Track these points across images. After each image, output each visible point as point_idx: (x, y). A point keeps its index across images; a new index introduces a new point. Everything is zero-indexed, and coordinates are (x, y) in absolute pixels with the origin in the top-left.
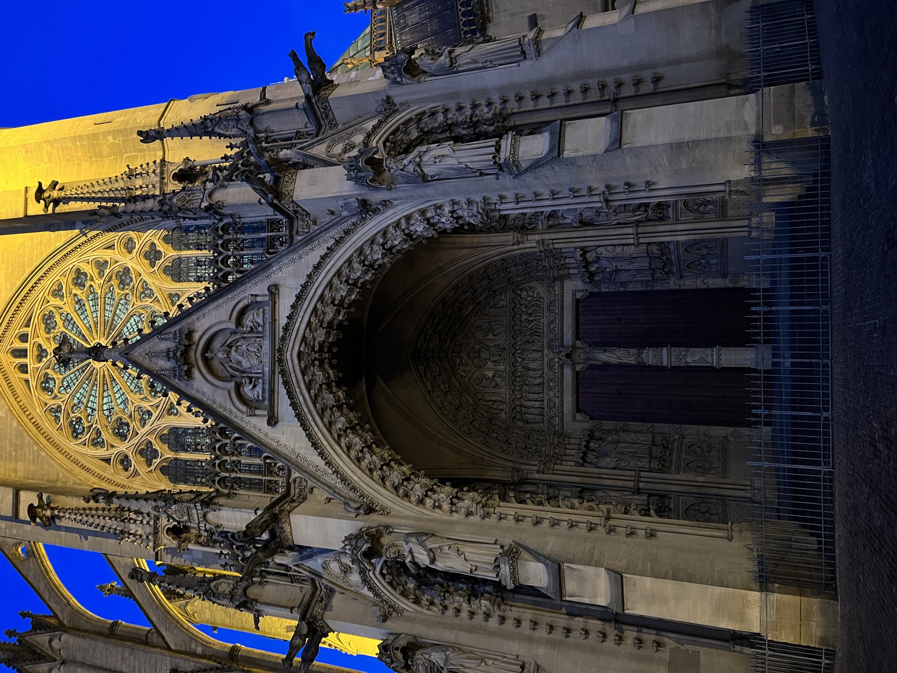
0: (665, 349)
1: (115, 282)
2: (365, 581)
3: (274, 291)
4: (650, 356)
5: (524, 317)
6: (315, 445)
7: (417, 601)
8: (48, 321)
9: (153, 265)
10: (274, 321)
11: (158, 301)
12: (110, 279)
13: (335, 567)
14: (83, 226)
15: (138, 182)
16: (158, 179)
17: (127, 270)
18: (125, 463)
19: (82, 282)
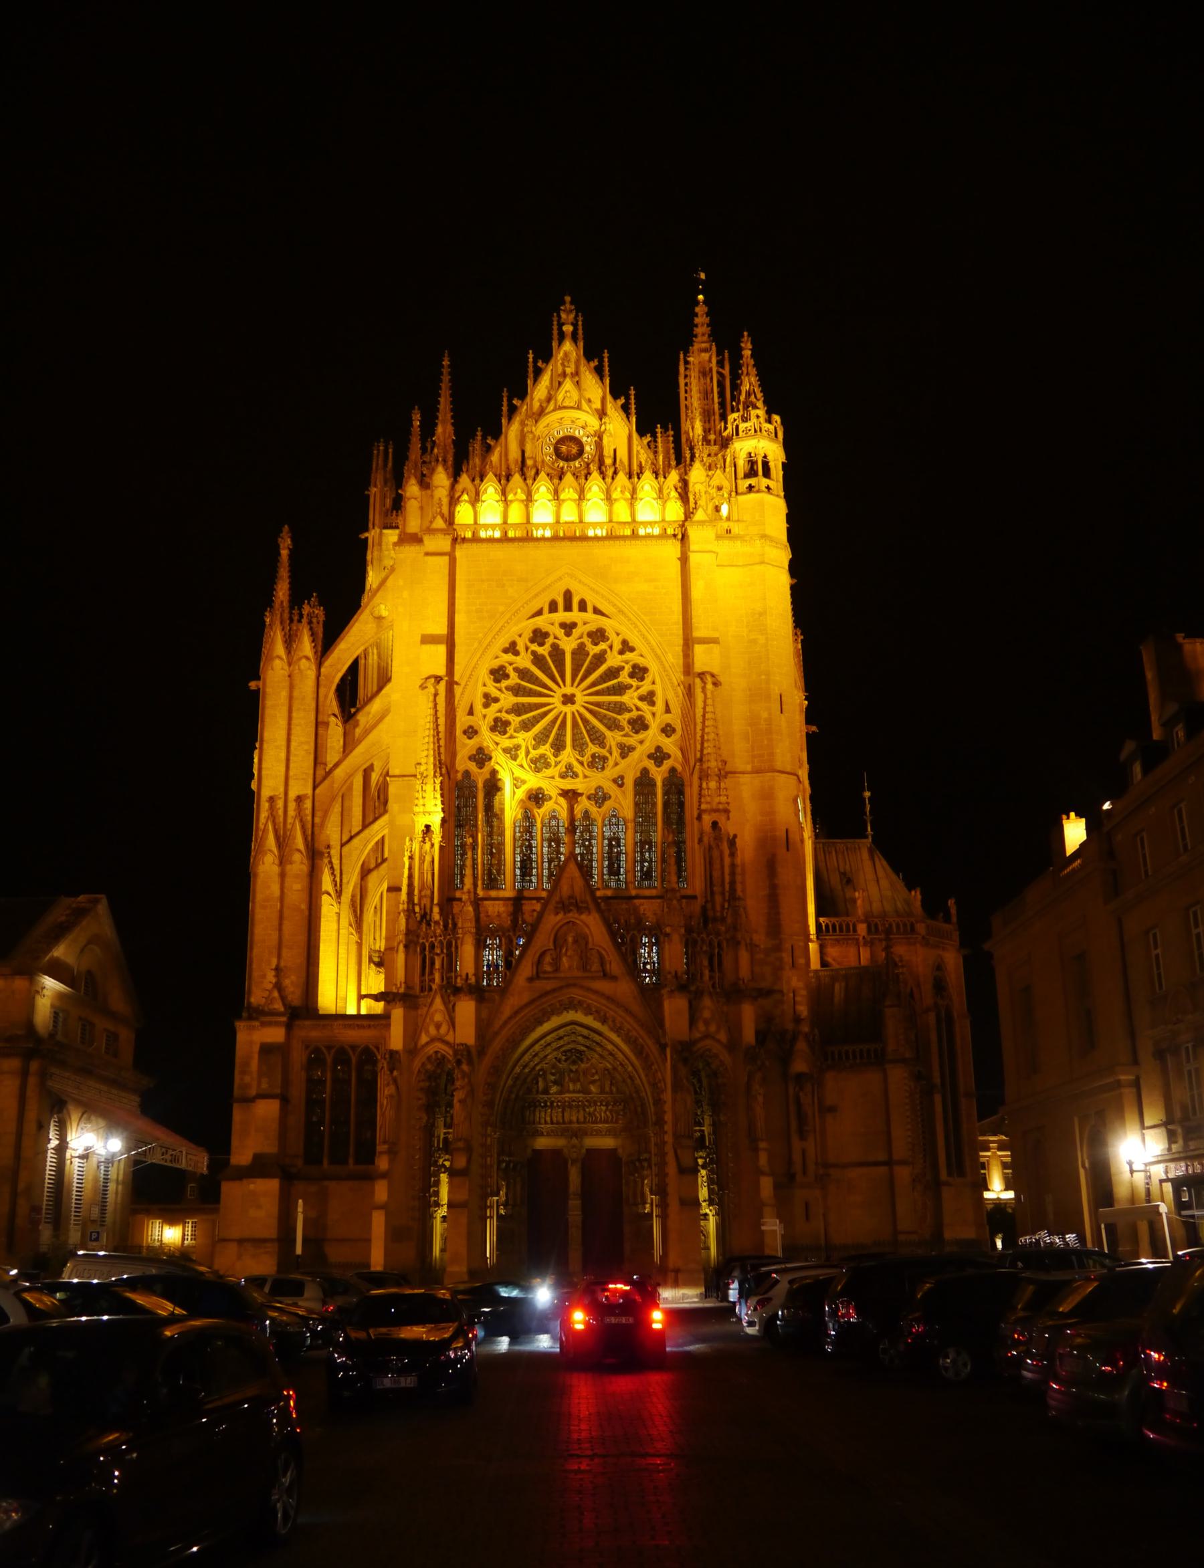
0: (580, 1213)
1: (635, 714)
2: (432, 1040)
3: (614, 978)
4: (574, 1204)
5: (604, 1108)
6: (516, 1013)
7: (419, 1071)
8: (599, 635)
9: (650, 756)
10: (593, 978)
11: (616, 764)
12: (638, 709)
13: (438, 1017)
14: (687, 685)
15: (713, 784)
16: (714, 806)
17: (646, 727)
18: (470, 730)
19: (636, 673)
